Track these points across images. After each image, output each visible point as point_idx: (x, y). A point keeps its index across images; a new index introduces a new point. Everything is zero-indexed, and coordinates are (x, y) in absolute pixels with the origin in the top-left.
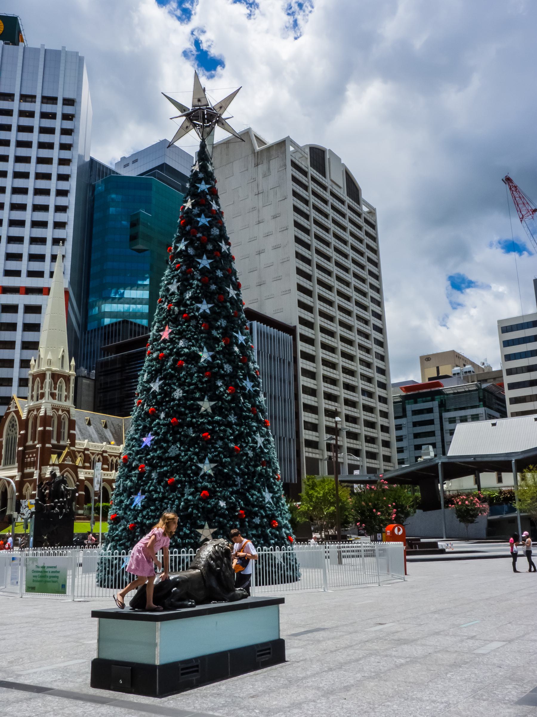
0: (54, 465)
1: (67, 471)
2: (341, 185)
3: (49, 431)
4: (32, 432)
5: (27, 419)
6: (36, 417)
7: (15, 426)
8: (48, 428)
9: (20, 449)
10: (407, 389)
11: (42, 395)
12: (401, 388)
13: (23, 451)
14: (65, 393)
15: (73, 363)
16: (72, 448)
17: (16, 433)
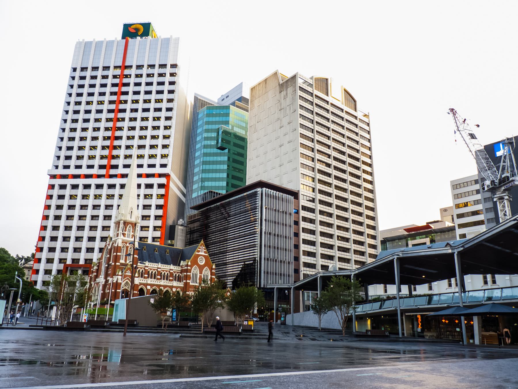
0: (118, 275)
1: (128, 279)
2: (340, 99)
3: (120, 256)
5: (111, 249)
8: (118, 254)
10: (407, 230)
12: (405, 230)
14: (132, 233)
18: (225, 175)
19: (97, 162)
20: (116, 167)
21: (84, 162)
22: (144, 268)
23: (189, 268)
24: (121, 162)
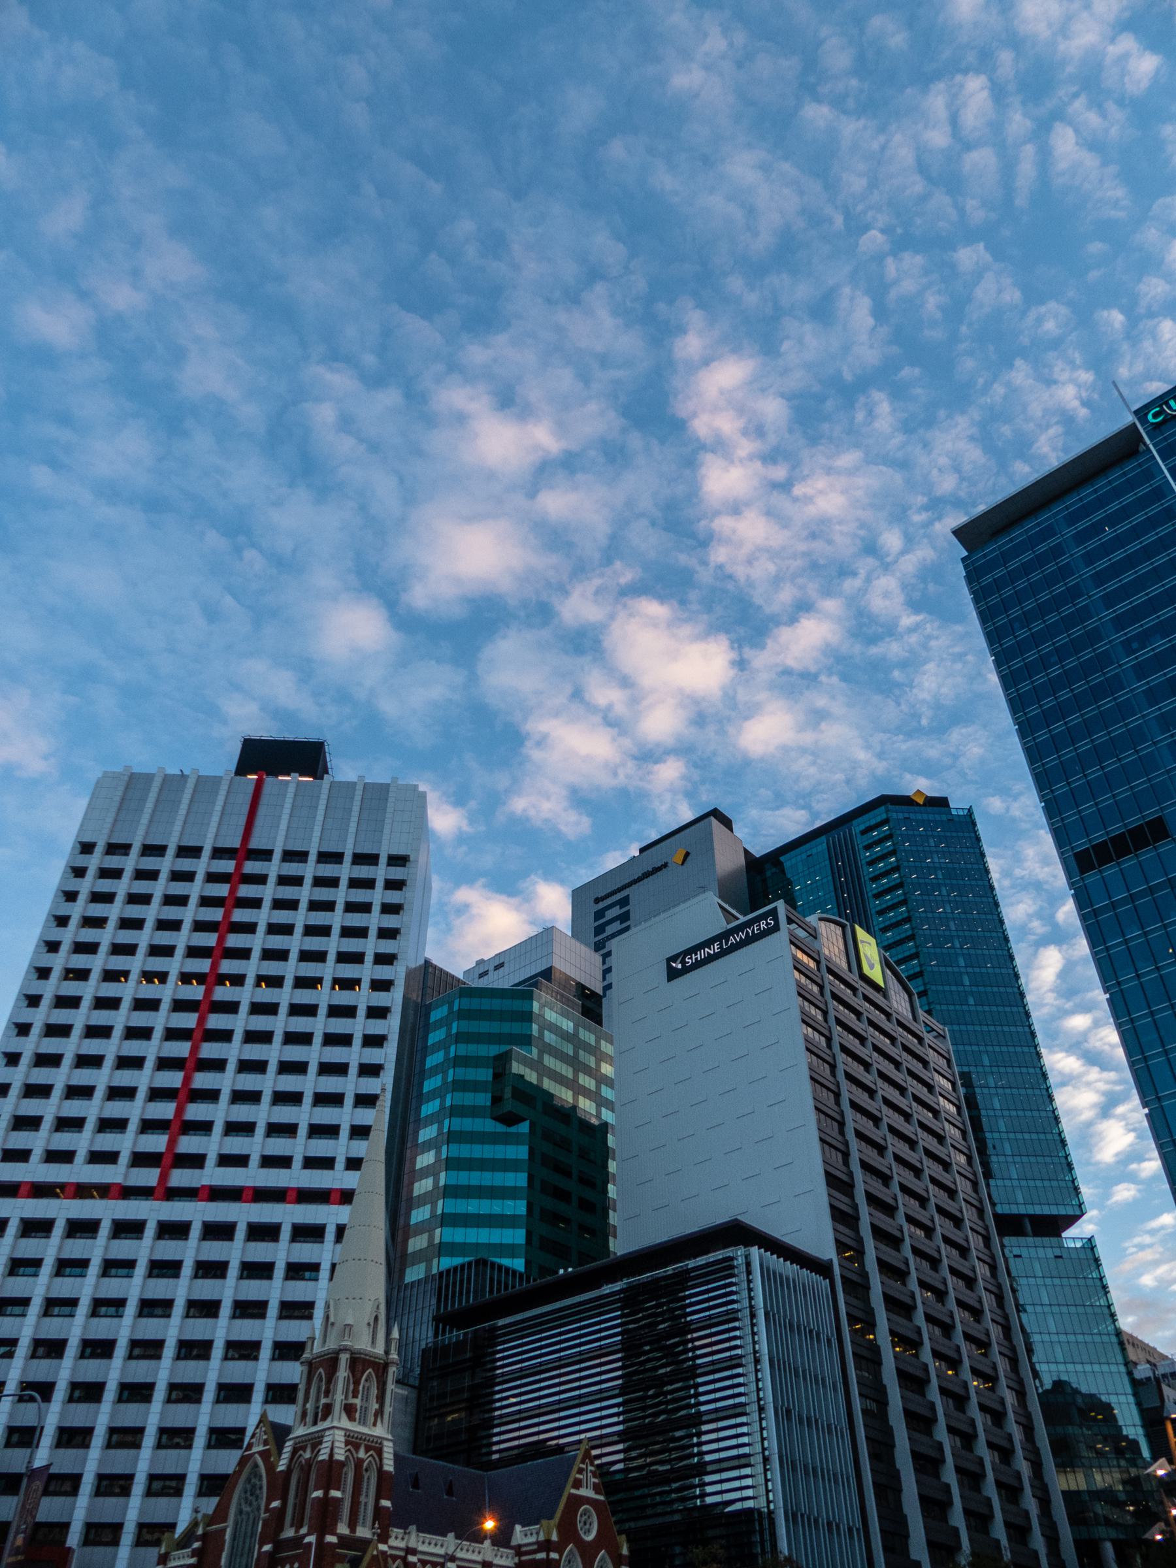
4: (295, 1505)
5: (289, 1472)
6: (309, 1462)
7: (258, 1492)
9: (267, 1548)
11: (328, 1410)
13: (270, 1554)
15: (395, 1334)
16: (383, 1547)
17: (259, 1509)
18: (520, 1207)
19: (125, 1143)
20: (196, 1161)
21: (82, 1142)
22: (404, 1559)
23: (554, 1556)
24: (212, 1145)
